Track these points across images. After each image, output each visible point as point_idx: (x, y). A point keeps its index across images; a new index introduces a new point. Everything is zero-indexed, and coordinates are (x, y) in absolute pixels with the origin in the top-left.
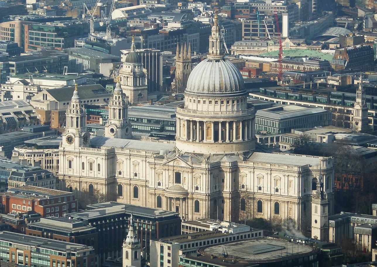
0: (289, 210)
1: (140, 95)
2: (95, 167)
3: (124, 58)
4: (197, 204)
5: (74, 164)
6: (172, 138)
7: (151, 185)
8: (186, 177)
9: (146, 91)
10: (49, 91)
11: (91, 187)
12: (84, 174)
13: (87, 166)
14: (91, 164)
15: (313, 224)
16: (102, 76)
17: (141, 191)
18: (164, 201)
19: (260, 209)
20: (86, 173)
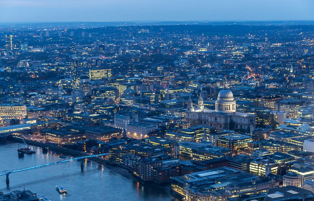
0: (244, 127)
1: (206, 98)
2: (195, 116)
3: (201, 89)
4: (221, 126)
5: (189, 115)
6: (214, 109)
7: (209, 120)
8: (218, 119)
9: (207, 97)
10: (183, 97)
11: (194, 121)
12: (192, 118)
13: (193, 116)
14: (194, 115)
15: (251, 130)
16: (196, 93)
17: (207, 123)
18: (212, 124)
19: (237, 127)
20: (193, 118)
